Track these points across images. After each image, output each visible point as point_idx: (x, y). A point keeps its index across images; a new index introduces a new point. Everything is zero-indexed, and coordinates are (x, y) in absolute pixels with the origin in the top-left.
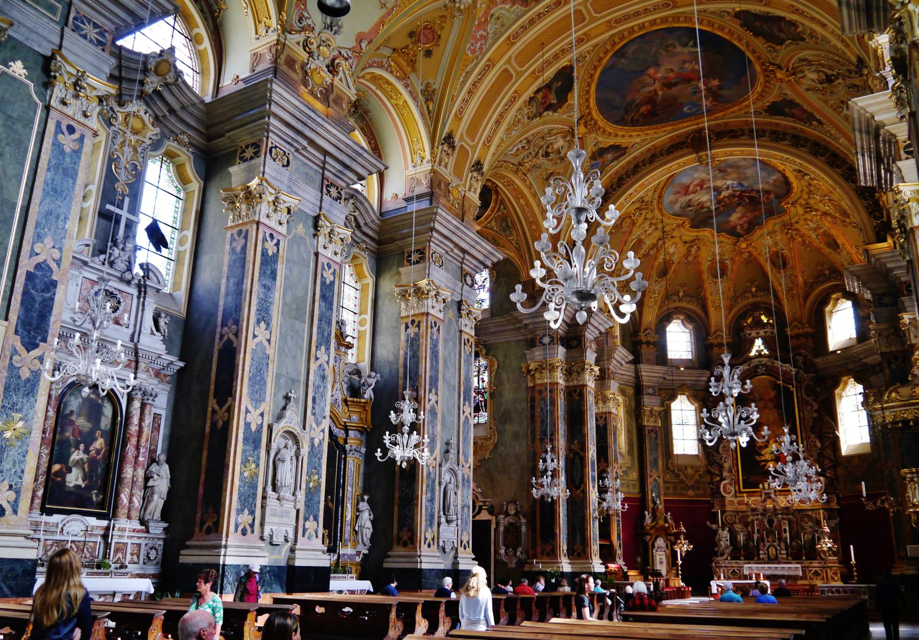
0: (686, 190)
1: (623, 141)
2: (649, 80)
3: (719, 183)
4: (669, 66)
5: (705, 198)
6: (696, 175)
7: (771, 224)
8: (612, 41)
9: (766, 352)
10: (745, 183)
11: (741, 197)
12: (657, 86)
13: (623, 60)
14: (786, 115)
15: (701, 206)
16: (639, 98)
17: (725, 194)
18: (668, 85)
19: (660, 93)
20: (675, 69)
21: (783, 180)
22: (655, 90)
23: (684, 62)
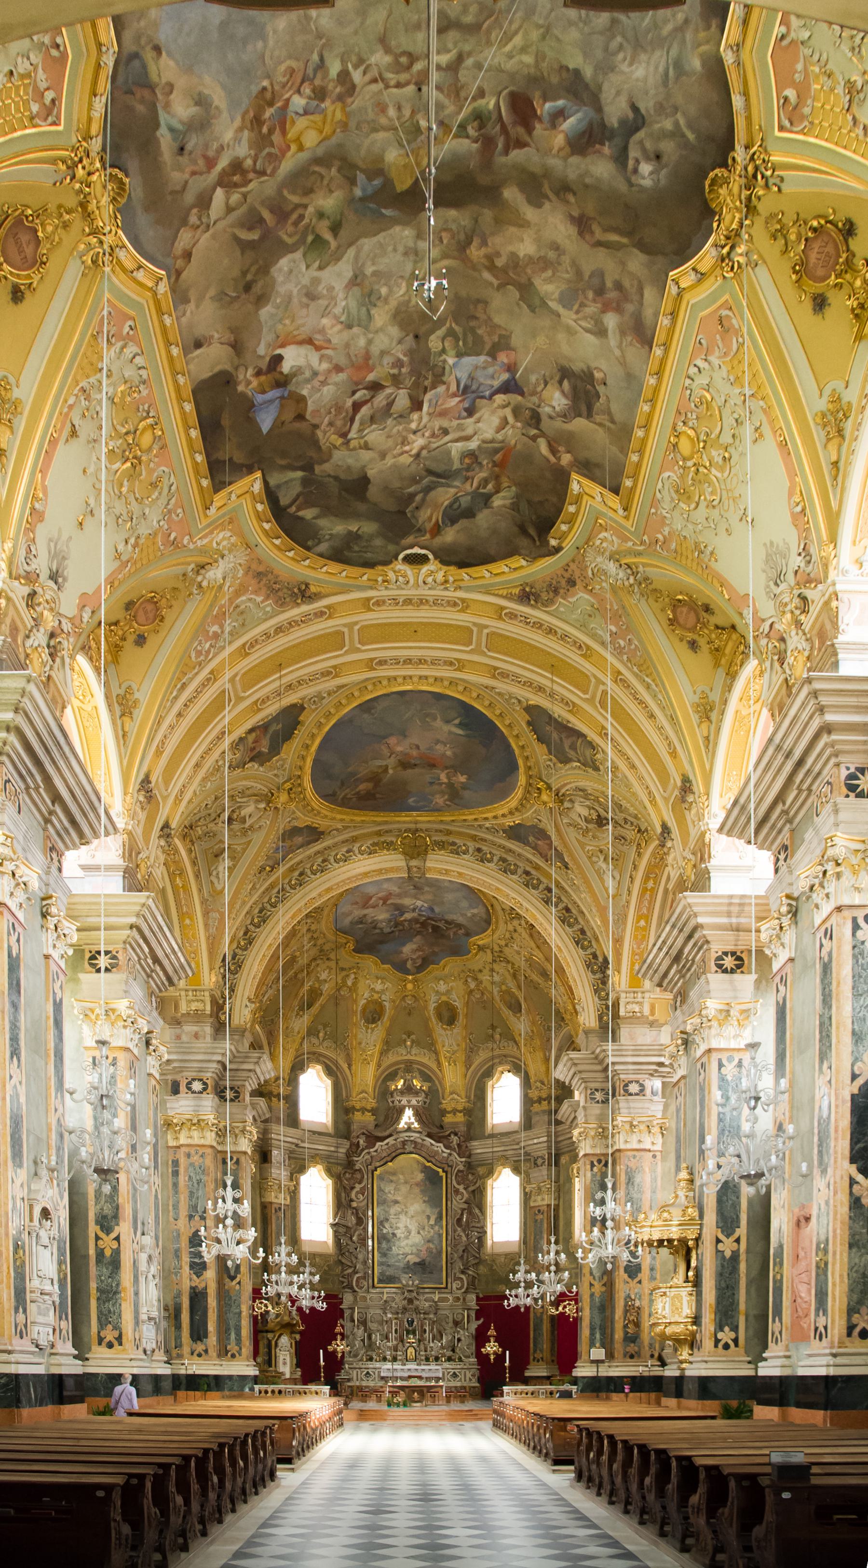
0: (366, 902)
1: (321, 823)
2: (386, 752)
3: (407, 902)
4: (415, 740)
5: (382, 916)
6: (385, 886)
7: (450, 965)
8: (362, 686)
9: (416, 1125)
10: (437, 910)
11: (424, 924)
12: (391, 762)
13: (366, 716)
14: (526, 843)
15: (374, 925)
16: (364, 771)
17: (408, 916)
18: (405, 764)
19: (391, 771)
20: (423, 748)
21: (484, 916)
22: (387, 767)
23: (438, 742)
